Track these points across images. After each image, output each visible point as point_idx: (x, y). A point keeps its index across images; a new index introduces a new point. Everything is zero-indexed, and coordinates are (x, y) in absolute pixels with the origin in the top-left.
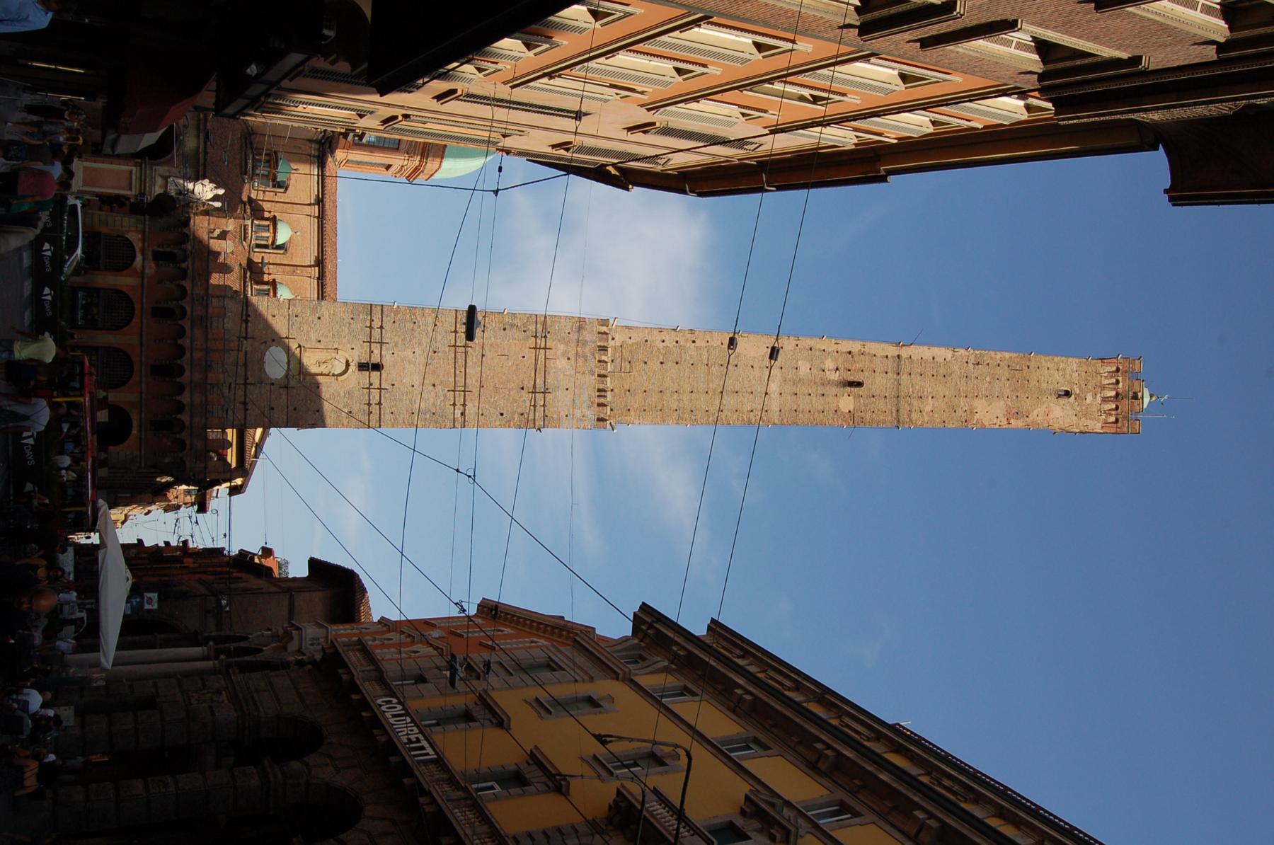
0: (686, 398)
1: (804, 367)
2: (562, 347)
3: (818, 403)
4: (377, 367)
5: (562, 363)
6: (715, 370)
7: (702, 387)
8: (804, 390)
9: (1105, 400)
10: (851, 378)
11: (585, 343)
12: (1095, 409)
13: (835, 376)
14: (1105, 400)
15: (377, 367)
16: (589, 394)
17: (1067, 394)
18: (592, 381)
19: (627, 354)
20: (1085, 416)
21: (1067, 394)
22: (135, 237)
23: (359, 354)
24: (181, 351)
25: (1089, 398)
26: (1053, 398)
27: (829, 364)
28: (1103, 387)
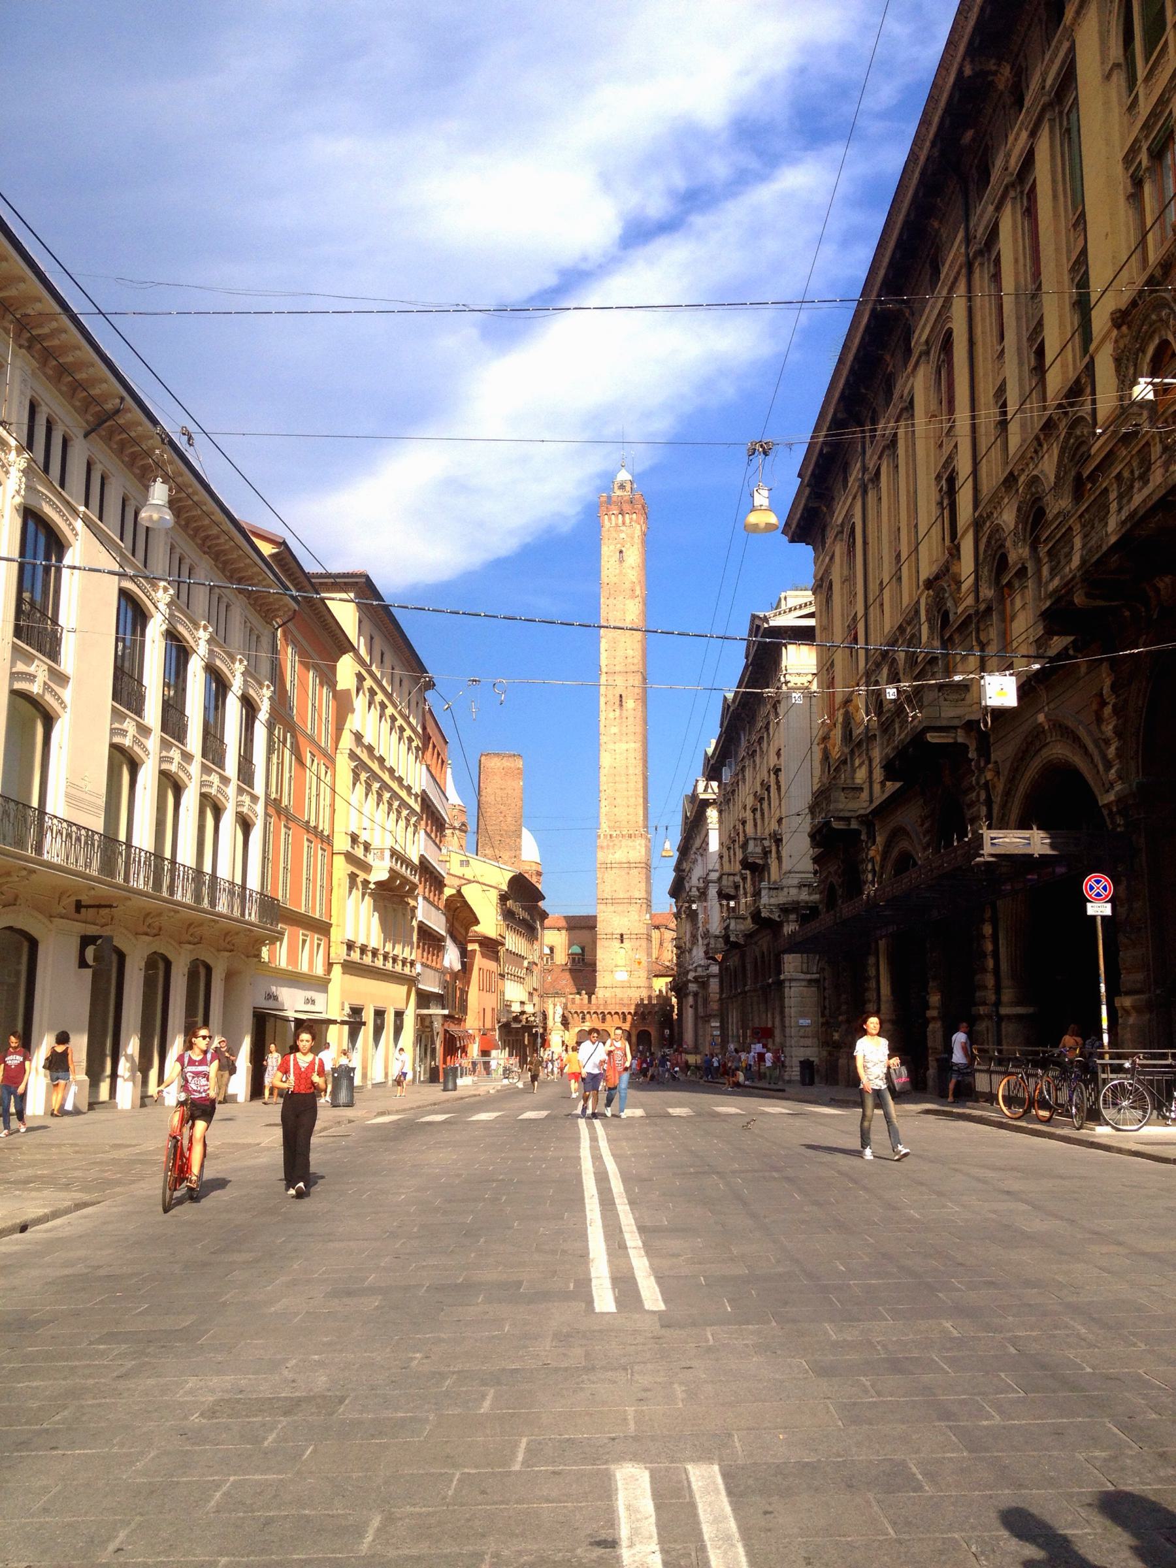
0: (631, 793)
1: (614, 730)
2: (610, 856)
3: (631, 719)
4: (622, 935)
6: (617, 779)
7: (625, 786)
8: (624, 729)
9: (624, 523)
10: (618, 703)
11: (608, 846)
12: (629, 531)
13: (618, 711)
14: (624, 523)
15: (622, 935)
16: (630, 843)
17: (621, 552)
18: (624, 842)
19: (612, 824)
20: (632, 538)
21: (621, 552)
22: (577, 1029)
23: (617, 943)
24: (616, 1013)
25: (623, 535)
26: (624, 564)
27: (612, 715)
28: (617, 525)
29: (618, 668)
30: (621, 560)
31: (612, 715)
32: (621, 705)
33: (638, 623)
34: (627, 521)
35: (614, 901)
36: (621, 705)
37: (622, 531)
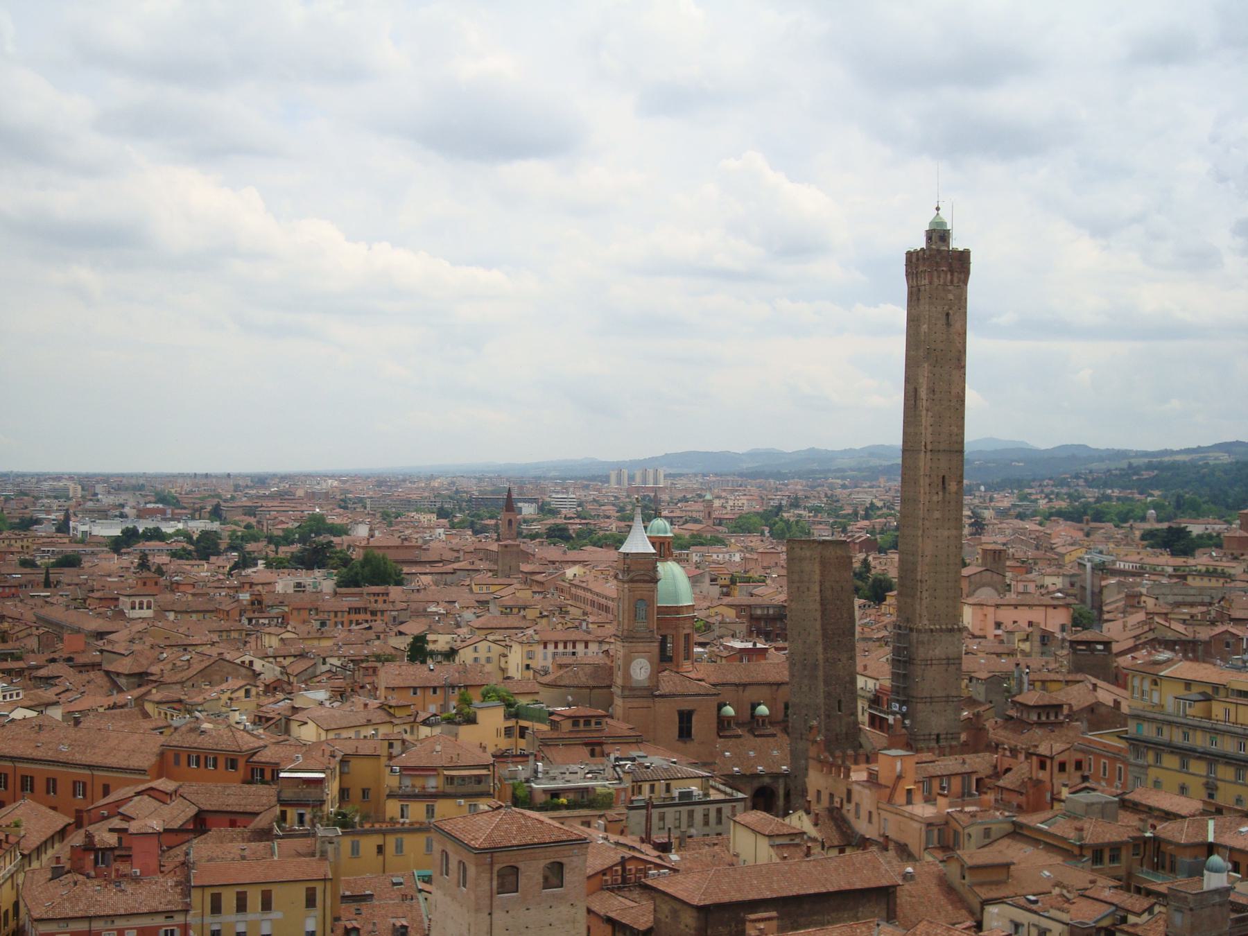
1: (937, 515)
5: (937, 652)
9: (952, 282)
14: (952, 282)
15: (938, 735)
21: (948, 314)
25: (951, 296)
27: (935, 498)
28: (945, 284)
29: (942, 447)
30: (948, 324)
31: (935, 498)
32: (944, 488)
33: (1001, 413)
34: (956, 280)
35: (932, 700)
36: (944, 488)
37: (949, 291)
